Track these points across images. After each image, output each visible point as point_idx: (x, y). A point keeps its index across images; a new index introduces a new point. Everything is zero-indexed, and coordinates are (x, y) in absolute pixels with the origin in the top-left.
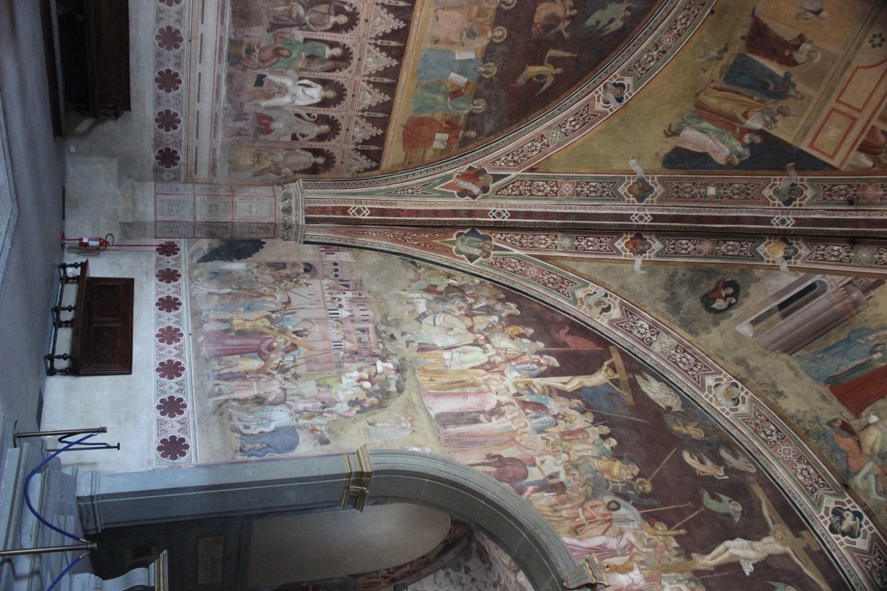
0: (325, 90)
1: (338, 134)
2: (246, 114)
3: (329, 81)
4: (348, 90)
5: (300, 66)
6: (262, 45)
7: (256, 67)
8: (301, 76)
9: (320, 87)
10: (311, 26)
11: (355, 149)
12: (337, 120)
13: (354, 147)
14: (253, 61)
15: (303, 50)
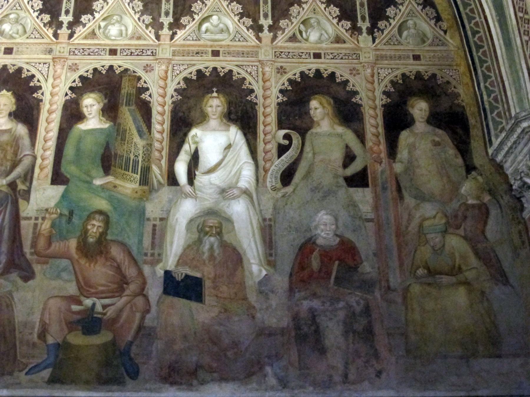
0: (203, 118)
1: (333, 74)
2: (296, 318)
3: (175, 112)
4: (201, 67)
5: (135, 186)
6: (72, 289)
7: (140, 301)
8: (163, 180)
9: (195, 132)
10: (19, 170)
11: (370, 31)
12: (290, 81)
13: (365, 39)
14: (121, 311)
15: (90, 183)
